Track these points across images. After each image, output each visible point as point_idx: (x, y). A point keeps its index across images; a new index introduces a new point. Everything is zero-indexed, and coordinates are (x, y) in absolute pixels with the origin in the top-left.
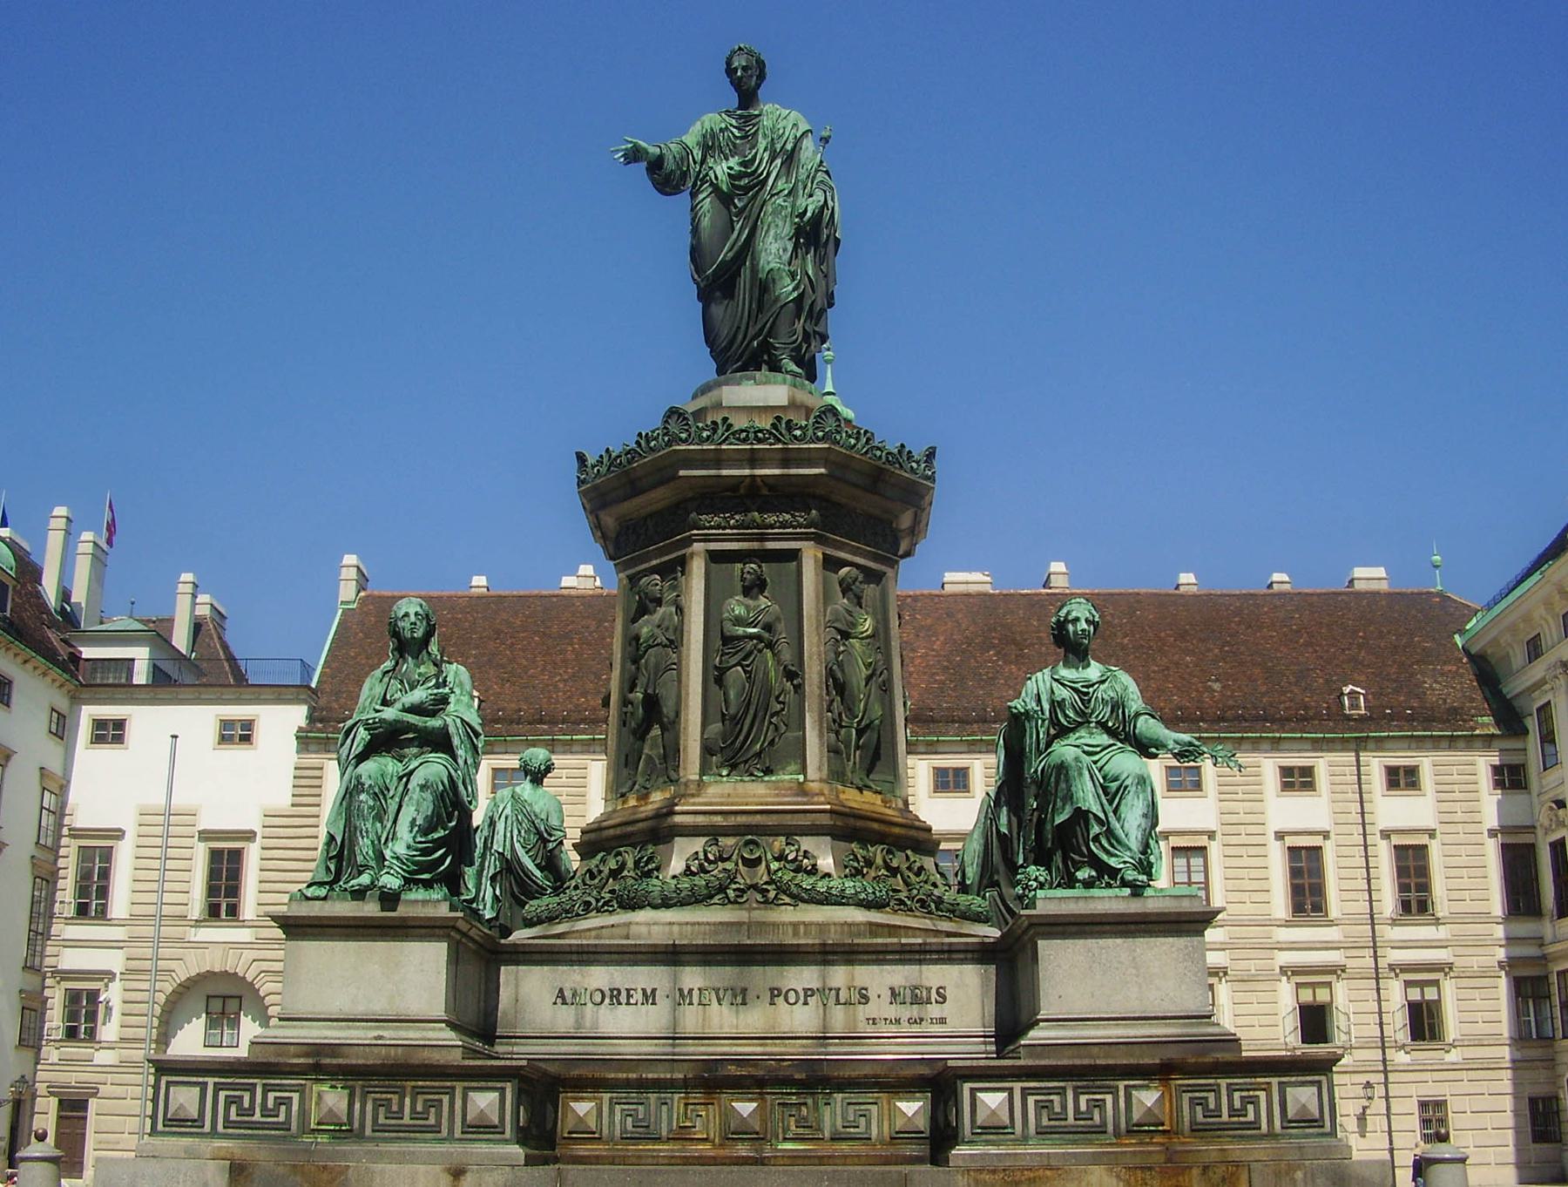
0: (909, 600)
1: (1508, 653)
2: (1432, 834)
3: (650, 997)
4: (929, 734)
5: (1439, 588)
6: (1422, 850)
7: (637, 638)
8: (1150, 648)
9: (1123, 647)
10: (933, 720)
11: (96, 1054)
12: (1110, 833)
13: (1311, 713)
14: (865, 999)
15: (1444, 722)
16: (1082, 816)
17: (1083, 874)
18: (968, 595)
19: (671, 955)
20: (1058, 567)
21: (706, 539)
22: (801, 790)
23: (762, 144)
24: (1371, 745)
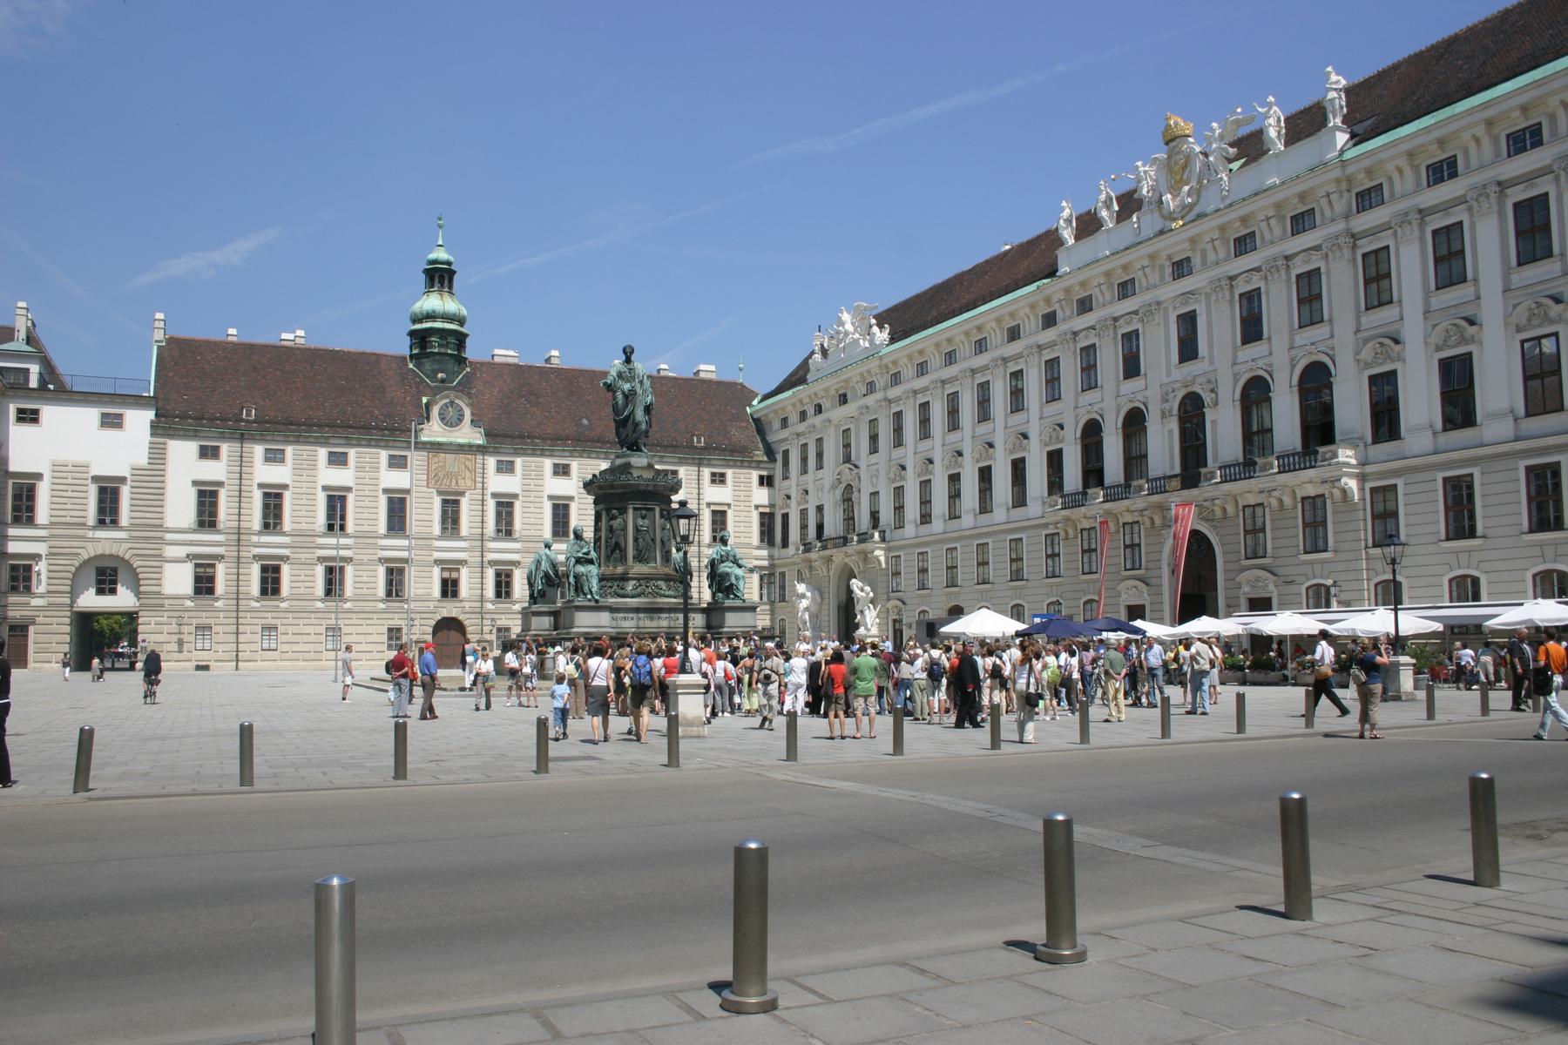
0: (478, 365)
1: (771, 422)
2: (729, 505)
3: (632, 619)
4: (497, 443)
5: (741, 381)
6: (724, 513)
7: (611, 527)
8: (602, 403)
9: (588, 401)
10: (497, 436)
11: (32, 600)
12: (737, 588)
13: (679, 444)
14: (678, 619)
15: (739, 452)
16: (732, 585)
17: (732, 596)
18: (509, 365)
19: (637, 610)
20: (555, 353)
21: (632, 504)
22: (655, 568)
23: (637, 381)
24: (705, 462)
